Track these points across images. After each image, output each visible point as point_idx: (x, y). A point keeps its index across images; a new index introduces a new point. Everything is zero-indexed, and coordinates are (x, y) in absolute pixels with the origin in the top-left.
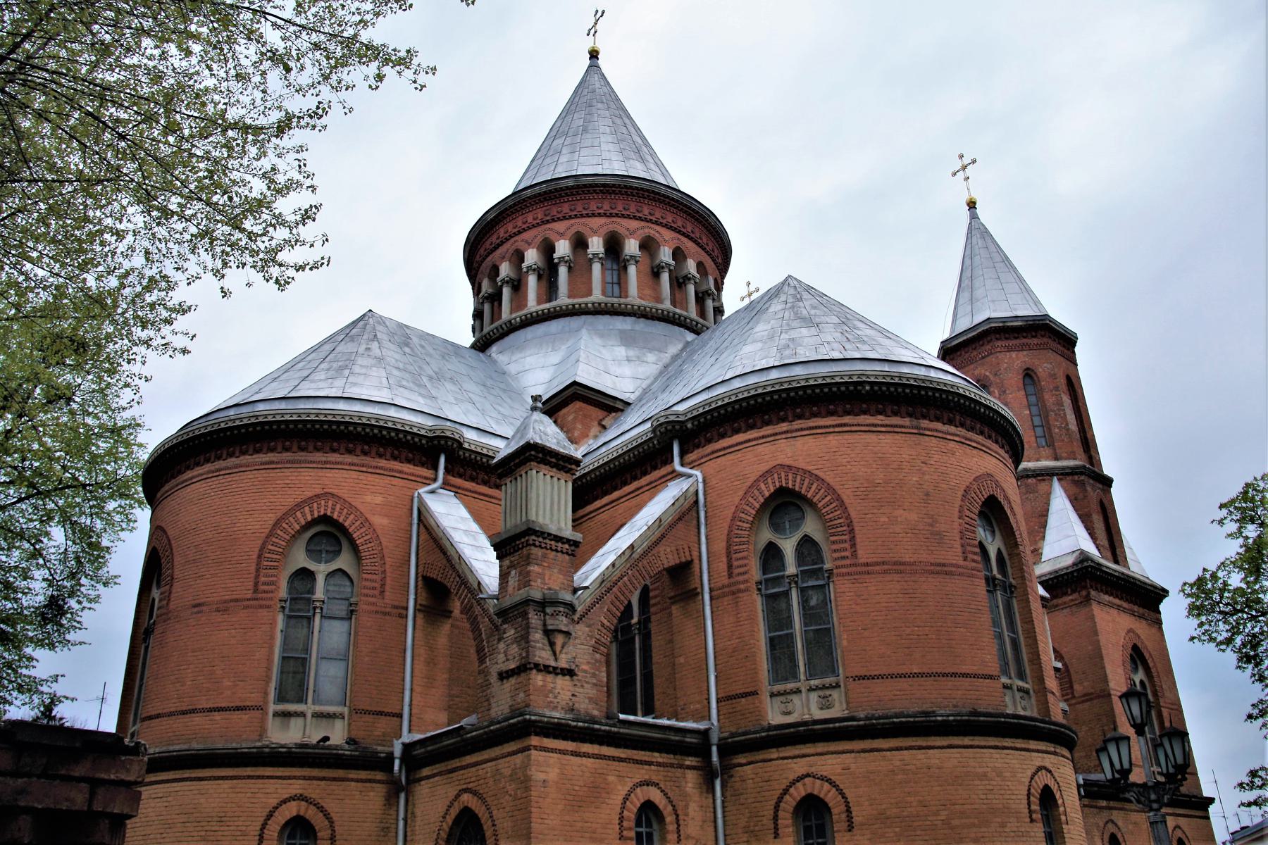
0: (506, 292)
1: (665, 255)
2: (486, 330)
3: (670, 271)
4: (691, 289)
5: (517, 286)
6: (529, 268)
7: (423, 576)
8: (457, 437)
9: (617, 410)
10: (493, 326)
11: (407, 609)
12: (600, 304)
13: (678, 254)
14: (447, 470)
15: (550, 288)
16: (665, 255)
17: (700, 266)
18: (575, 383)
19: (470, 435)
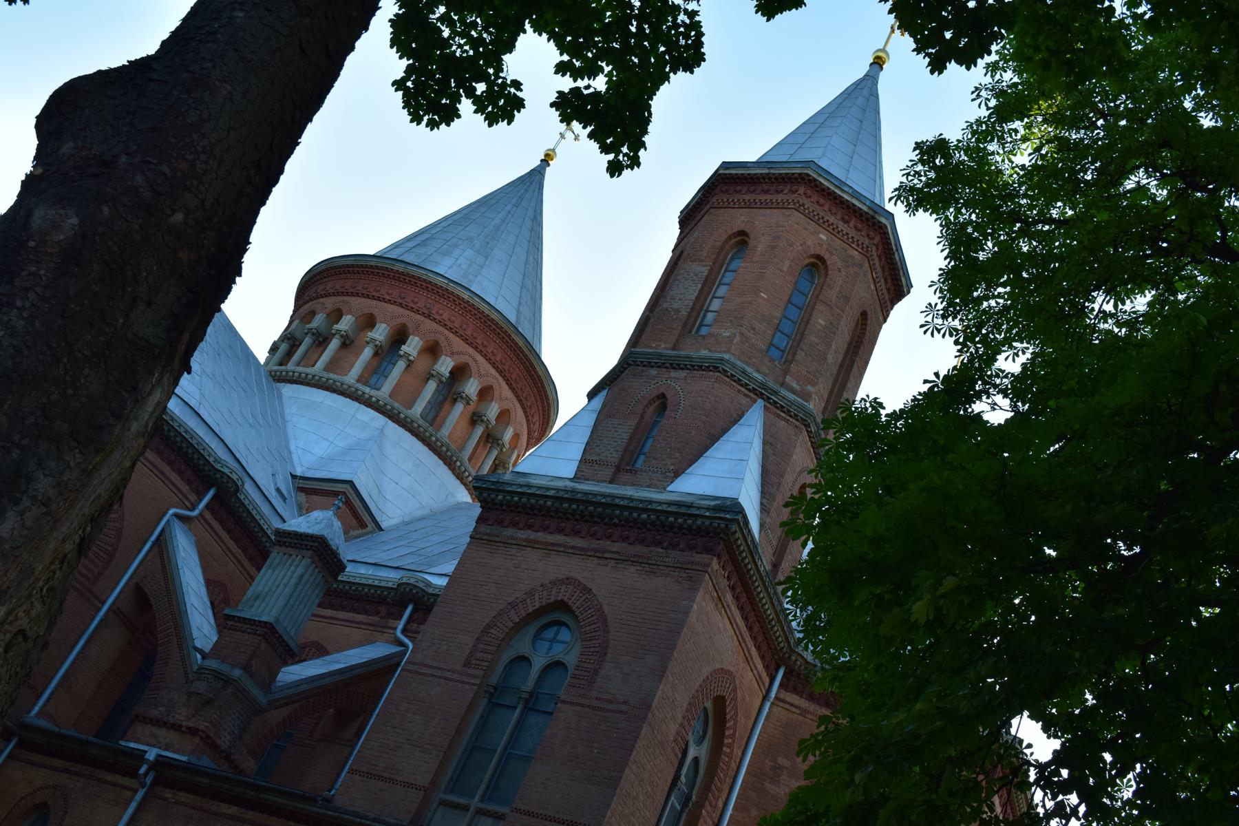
0: (335, 344)
1: (492, 411)
2: (291, 366)
3: (487, 427)
4: (495, 453)
5: (347, 343)
6: (373, 340)
7: (137, 584)
8: (240, 483)
9: (363, 525)
10: (300, 369)
11: (103, 603)
12: (412, 421)
13: (504, 415)
14: (207, 506)
15: (376, 371)
16: (492, 411)
17: (516, 436)
18: (351, 483)
19: (249, 487)
